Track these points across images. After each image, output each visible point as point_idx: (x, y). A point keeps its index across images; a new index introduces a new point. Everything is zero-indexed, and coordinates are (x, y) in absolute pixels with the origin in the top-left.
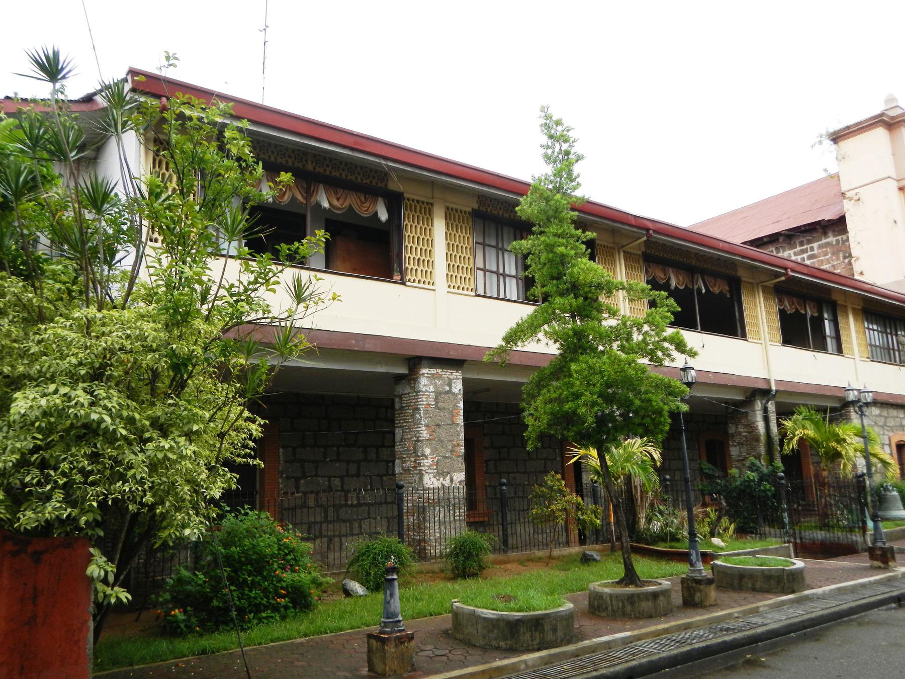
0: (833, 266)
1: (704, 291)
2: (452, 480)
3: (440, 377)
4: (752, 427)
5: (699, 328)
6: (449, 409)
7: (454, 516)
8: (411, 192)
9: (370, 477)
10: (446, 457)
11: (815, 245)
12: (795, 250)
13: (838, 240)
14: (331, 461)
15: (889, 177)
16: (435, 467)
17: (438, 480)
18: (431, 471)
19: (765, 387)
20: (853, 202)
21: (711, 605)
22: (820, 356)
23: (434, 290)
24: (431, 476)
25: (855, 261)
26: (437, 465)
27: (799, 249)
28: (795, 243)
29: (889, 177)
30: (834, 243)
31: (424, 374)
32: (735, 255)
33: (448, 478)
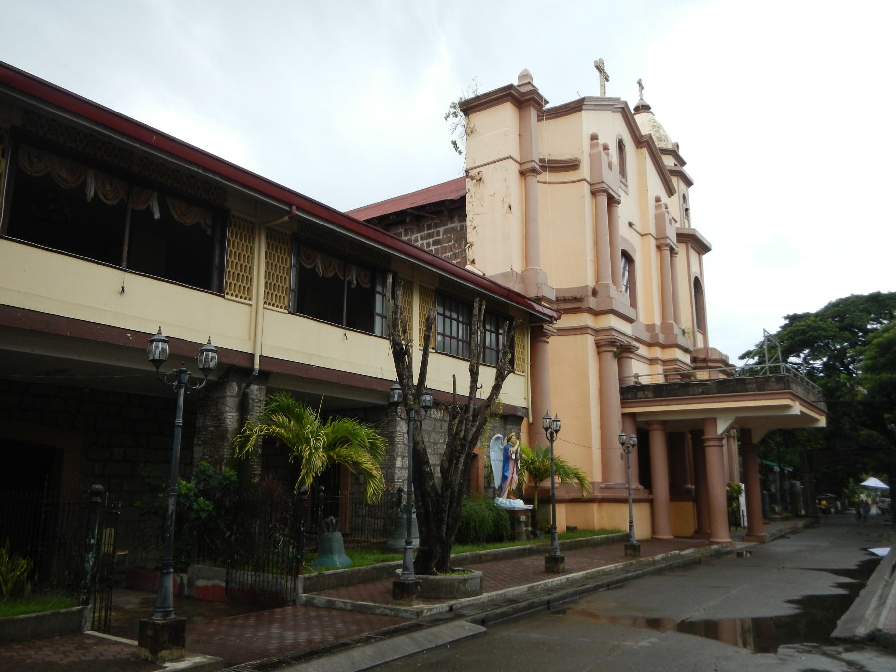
0: (455, 254)
1: (157, 215)
4: (219, 419)
5: (125, 264)
11: (441, 230)
12: (422, 234)
13: (463, 225)
15: (510, 157)
19: (245, 364)
20: (475, 181)
22: (356, 337)
25: (469, 247)
27: (426, 232)
28: (423, 225)
29: (510, 157)
30: (459, 229)
32: (191, 163)
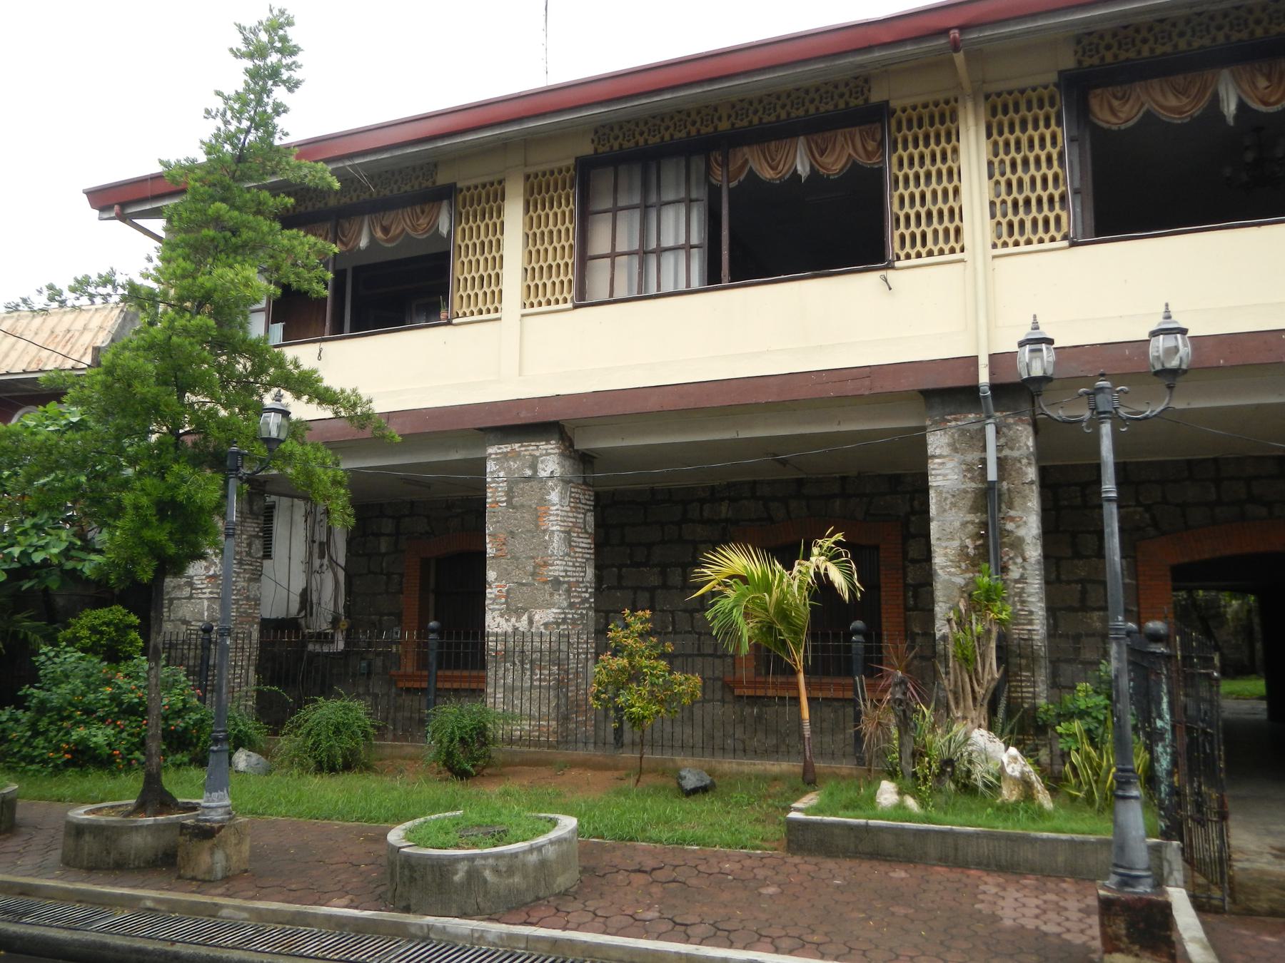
2: (531, 622)
3: (517, 456)
6: (530, 507)
7: (531, 679)
8: (466, 177)
9: (672, 612)
10: (524, 585)
14: (609, 588)
16: (503, 600)
17: (507, 620)
18: (497, 607)
21: (193, 879)
23: (499, 319)
24: (496, 613)
26: (507, 597)
31: (491, 454)
33: (525, 617)
